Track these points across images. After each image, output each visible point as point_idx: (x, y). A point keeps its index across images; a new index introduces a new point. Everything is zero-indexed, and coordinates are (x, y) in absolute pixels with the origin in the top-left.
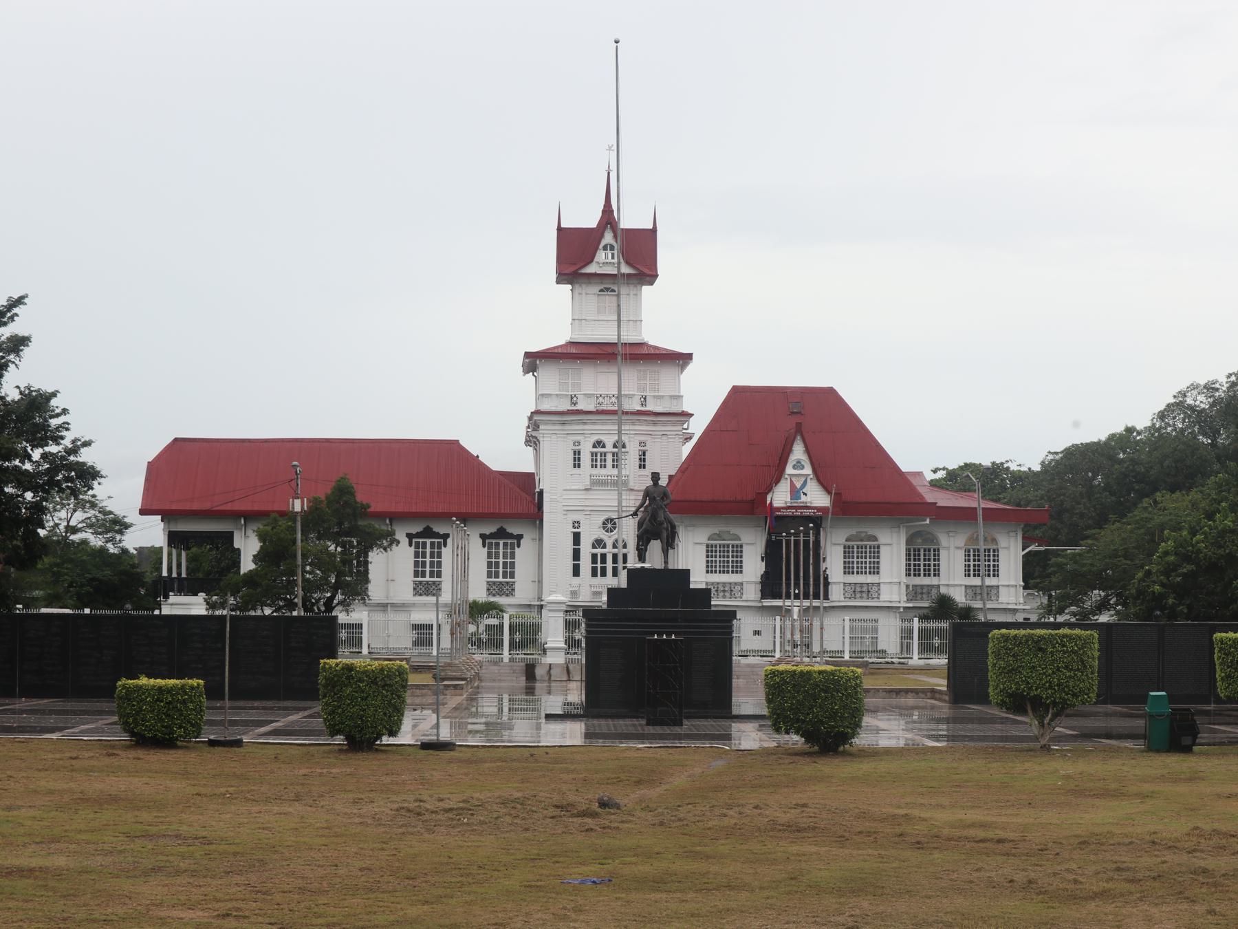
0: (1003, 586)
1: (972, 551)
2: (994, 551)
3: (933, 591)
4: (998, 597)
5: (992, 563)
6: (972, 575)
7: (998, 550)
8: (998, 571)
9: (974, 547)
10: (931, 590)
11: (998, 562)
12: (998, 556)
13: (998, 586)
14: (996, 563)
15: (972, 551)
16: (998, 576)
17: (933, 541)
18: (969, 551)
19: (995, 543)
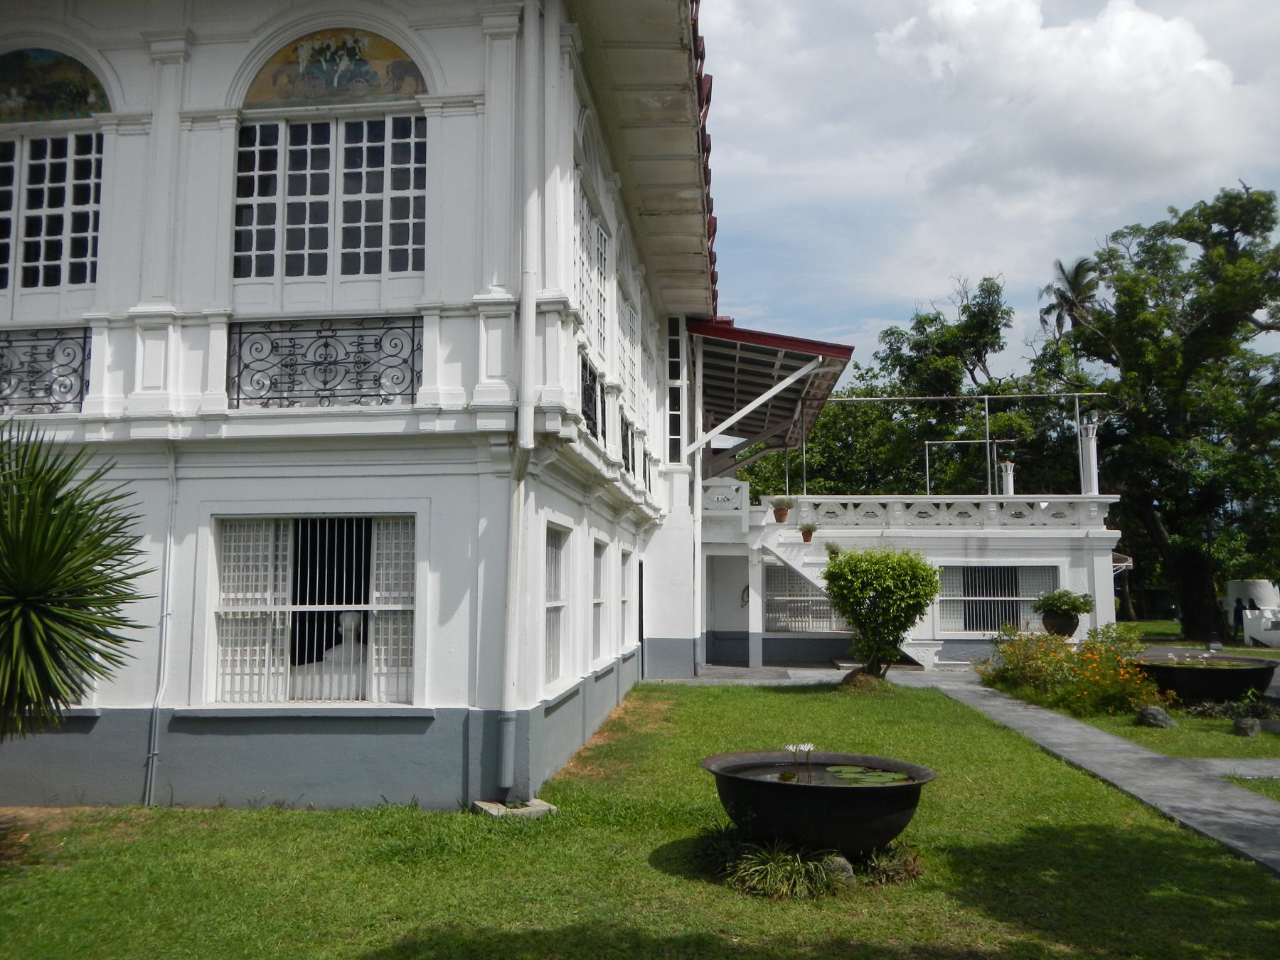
0: (444, 312)
1: (283, 133)
2: (402, 128)
3: (61, 358)
4: (416, 378)
5: (388, 194)
6: (279, 265)
7: (421, 121)
8: (420, 236)
9: (297, 111)
10: (51, 355)
11: (421, 183)
12: (421, 150)
13: (415, 320)
14: (411, 193)
15: (283, 133)
16: (419, 265)
17: (86, 94)
18: (270, 135)
19: (409, 82)
